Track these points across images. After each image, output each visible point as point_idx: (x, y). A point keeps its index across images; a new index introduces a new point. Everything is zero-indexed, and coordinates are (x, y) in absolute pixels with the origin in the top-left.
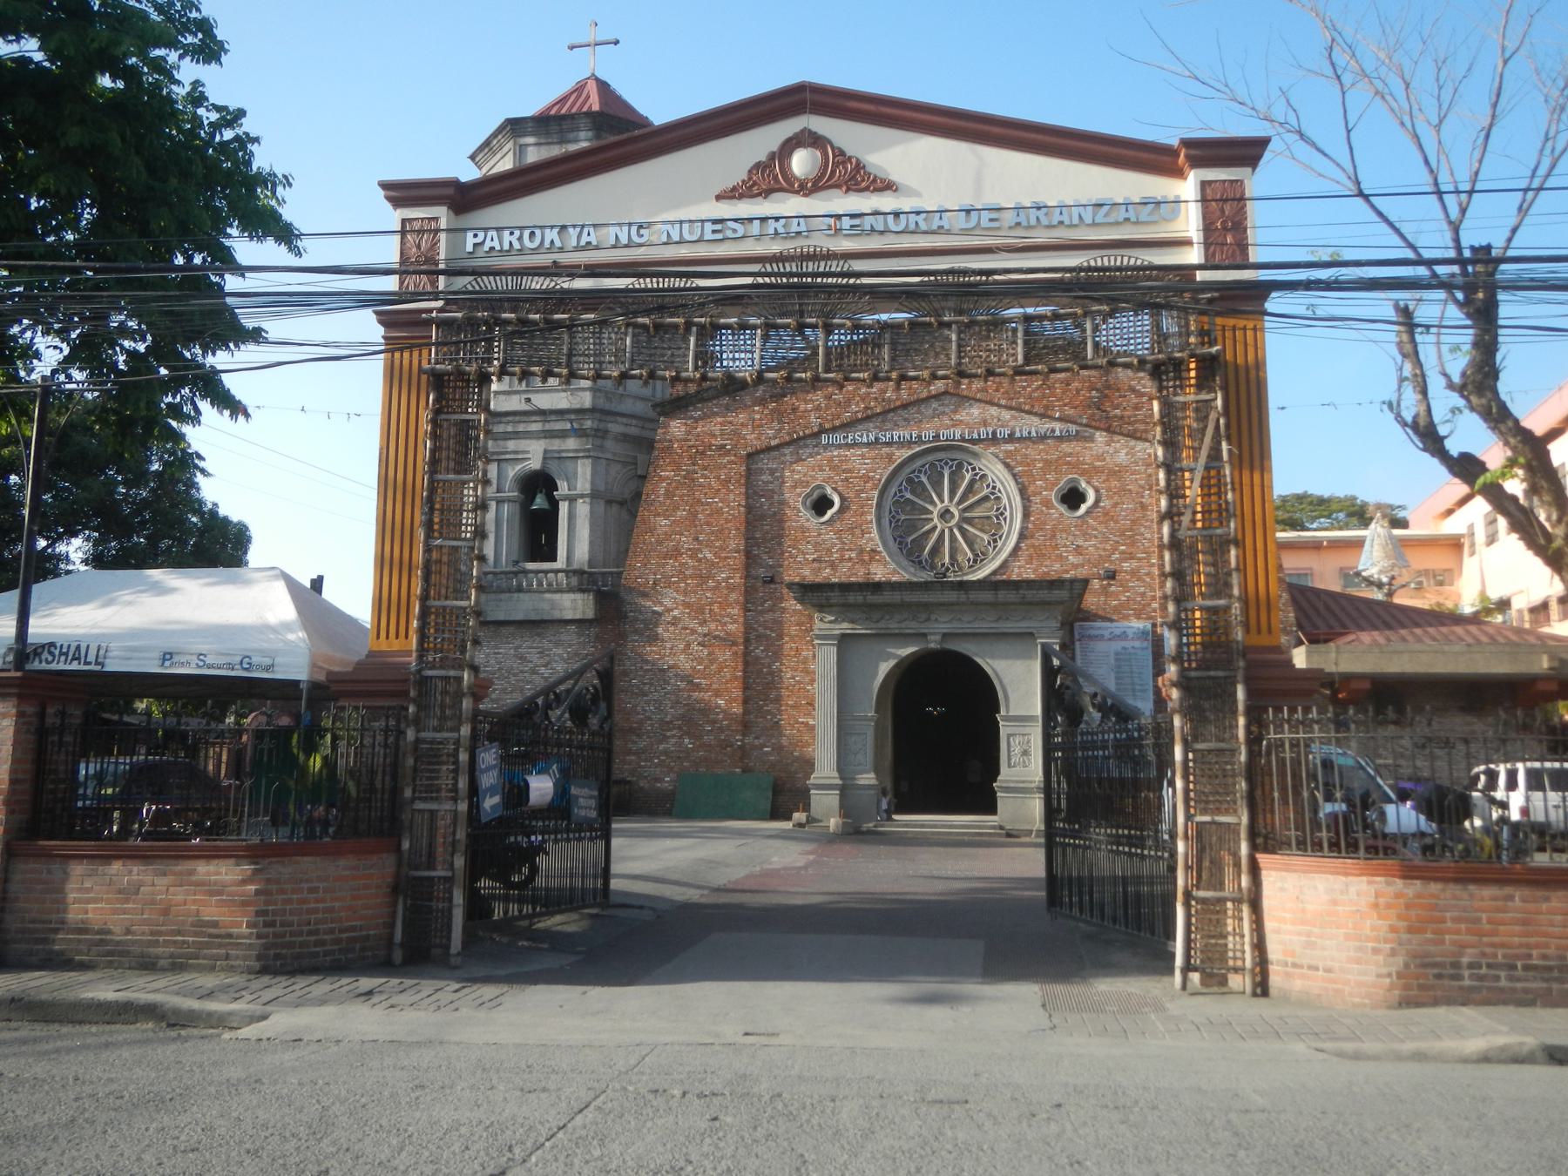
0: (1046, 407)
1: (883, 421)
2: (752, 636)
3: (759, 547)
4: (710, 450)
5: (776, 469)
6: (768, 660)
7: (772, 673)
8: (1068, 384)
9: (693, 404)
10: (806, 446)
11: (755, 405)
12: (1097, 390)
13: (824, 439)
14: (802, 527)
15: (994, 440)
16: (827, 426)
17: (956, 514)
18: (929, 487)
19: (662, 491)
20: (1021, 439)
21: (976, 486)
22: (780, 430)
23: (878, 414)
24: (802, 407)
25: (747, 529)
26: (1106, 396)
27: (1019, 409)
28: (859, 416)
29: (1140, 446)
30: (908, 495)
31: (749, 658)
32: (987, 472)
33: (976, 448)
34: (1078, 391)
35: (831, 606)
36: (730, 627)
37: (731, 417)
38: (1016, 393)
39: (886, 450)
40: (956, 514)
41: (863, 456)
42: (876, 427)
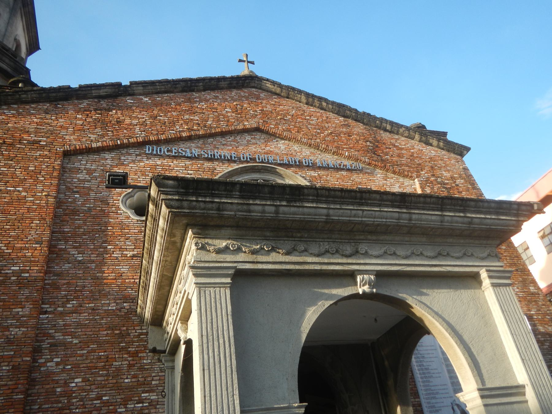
0: (338, 148)
1: (204, 143)
2: (45, 345)
3: (66, 241)
4: (20, 143)
5: (95, 170)
6: (64, 376)
7: (68, 394)
8: (351, 136)
10: (130, 154)
11: (78, 112)
12: (370, 142)
13: (148, 149)
14: (121, 224)
16: (152, 138)
20: (320, 168)
22: (103, 136)
23: (199, 137)
24: (128, 121)
25: (55, 223)
26: (377, 146)
27: (317, 147)
28: (184, 135)
31: (36, 375)
34: (358, 141)
35: (219, 227)
36: (14, 331)
37: (51, 119)
38: (312, 135)
39: (207, 164)
41: (186, 168)
42: (198, 147)
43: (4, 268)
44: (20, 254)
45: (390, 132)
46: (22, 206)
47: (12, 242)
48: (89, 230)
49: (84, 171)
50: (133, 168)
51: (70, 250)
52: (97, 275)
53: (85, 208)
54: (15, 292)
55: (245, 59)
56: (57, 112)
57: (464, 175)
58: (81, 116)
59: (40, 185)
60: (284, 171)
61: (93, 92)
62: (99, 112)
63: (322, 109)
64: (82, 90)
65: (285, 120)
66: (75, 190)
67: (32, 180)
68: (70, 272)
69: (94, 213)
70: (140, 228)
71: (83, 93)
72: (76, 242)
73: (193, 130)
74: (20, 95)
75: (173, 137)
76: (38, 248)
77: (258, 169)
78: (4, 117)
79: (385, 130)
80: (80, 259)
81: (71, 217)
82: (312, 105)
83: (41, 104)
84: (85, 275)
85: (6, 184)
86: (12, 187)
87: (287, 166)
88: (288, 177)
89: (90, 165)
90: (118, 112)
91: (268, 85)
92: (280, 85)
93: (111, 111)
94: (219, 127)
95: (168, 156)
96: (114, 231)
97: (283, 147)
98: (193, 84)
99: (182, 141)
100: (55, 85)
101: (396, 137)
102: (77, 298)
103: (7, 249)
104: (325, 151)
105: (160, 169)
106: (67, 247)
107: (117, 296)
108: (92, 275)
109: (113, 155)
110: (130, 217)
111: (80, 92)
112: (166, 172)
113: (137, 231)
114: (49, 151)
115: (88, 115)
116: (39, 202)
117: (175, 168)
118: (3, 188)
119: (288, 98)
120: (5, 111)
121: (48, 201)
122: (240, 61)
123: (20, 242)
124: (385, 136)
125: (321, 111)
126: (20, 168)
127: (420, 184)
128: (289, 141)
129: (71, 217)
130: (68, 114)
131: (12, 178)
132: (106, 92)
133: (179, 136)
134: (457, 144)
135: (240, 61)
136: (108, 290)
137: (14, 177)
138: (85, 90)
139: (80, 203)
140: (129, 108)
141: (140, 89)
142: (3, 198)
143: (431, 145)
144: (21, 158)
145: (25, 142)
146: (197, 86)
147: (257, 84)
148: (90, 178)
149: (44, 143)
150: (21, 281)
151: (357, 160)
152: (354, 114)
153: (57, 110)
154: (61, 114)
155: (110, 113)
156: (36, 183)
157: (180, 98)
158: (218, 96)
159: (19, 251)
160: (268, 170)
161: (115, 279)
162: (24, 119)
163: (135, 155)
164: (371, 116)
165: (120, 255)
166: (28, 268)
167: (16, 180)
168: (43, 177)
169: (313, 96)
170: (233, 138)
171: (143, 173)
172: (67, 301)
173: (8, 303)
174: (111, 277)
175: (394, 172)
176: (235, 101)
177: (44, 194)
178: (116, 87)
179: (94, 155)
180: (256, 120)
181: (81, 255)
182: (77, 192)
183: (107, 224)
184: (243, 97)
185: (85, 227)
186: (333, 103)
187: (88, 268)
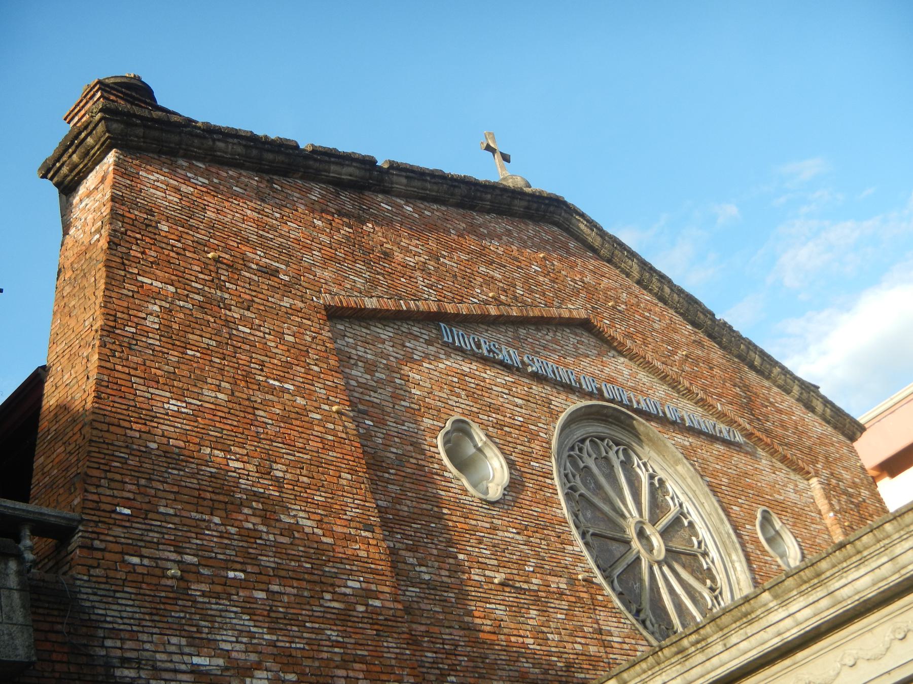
8: (711, 368)
9: (188, 156)
10: (416, 338)
14: (459, 504)
15: (663, 420)
16: (450, 308)
17: (657, 541)
18: (602, 480)
19: (152, 323)
21: (660, 499)
22: (373, 283)
27: (674, 385)
28: (493, 311)
29: (802, 484)
30: (583, 490)
32: (661, 474)
33: (653, 428)
39: (536, 389)
40: (657, 541)
42: (508, 344)
43: (337, 582)
44: (349, 552)
45: (759, 372)
46: (309, 432)
47: (326, 520)
48: (416, 511)
49: (360, 364)
50: (432, 372)
51: (403, 553)
52: (467, 619)
53: (392, 456)
54: (374, 643)
55: (492, 145)
56: (277, 201)
57: (865, 482)
58: (320, 223)
59: (319, 385)
60: (646, 426)
61: (333, 167)
62: (345, 220)
63: (662, 299)
64: (316, 160)
65: (620, 311)
66: (360, 407)
67: (303, 370)
68: (423, 606)
69: (409, 470)
70: (489, 520)
71: (317, 165)
72: (407, 537)
73: (502, 303)
74: (214, 140)
75: (479, 312)
76: (371, 541)
77: (606, 416)
78: (192, 189)
79: (752, 367)
80: (427, 577)
81: (379, 473)
82: (645, 288)
83: (244, 173)
84: (449, 617)
85: (262, 370)
86: (274, 379)
87: (647, 416)
88: (651, 440)
89: (363, 349)
90: (377, 229)
91: (582, 226)
92: (602, 233)
93: (364, 223)
94: (536, 306)
95: (474, 355)
96: (454, 518)
97: (626, 372)
98: (479, 194)
99: (482, 324)
100: (273, 136)
101: (767, 383)
102: (453, 668)
103: (324, 535)
104: (683, 395)
105: (473, 385)
106: (398, 545)
107: (511, 673)
108: (457, 618)
109: (391, 335)
110: (466, 491)
111: (311, 163)
112: (484, 394)
113: (488, 525)
114: (302, 301)
115: (331, 224)
116: (331, 426)
117: (495, 388)
118: (261, 378)
119: (609, 261)
120: (189, 175)
121: (345, 426)
122: (488, 148)
123: (339, 522)
124: (752, 376)
125: (660, 304)
126: (270, 334)
127: (824, 489)
128: (631, 359)
129: (379, 473)
130: (297, 210)
131: (267, 356)
132: (350, 175)
133: (487, 313)
134: (848, 416)
135: (488, 148)
136: (493, 657)
137: (269, 354)
138: (320, 161)
139: (380, 441)
140: (389, 223)
141: (400, 183)
142: (270, 404)
143: (812, 410)
144: (262, 308)
145: (254, 266)
146: (482, 199)
147: (563, 217)
148: (375, 384)
149: (287, 278)
150: (374, 616)
151: (731, 422)
152: (709, 323)
153: (275, 195)
154: (288, 210)
155: (365, 228)
156: (311, 377)
157: (458, 220)
158: (510, 230)
159: (344, 543)
160: (622, 422)
161: (494, 633)
162: (229, 204)
163: (421, 340)
164: (734, 331)
165: (483, 579)
166: (373, 587)
167: (276, 362)
168: (316, 365)
169: (652, 270)
170: (551, 334)
171: (451, 388)
172: (442, 675)
173: (372, 668)
174: (488, 628)
175: (784, 459)
176: (540, 249)
177: (335, 408)
178: (368, 167)
179: (360, 326)
180: (580, 302)
181: (423, 569)
182: (365, 413)
183: (437, 501)
184: (547, 242)
185: (408, 503)
186: (680, 291)
187: (445, 601)
